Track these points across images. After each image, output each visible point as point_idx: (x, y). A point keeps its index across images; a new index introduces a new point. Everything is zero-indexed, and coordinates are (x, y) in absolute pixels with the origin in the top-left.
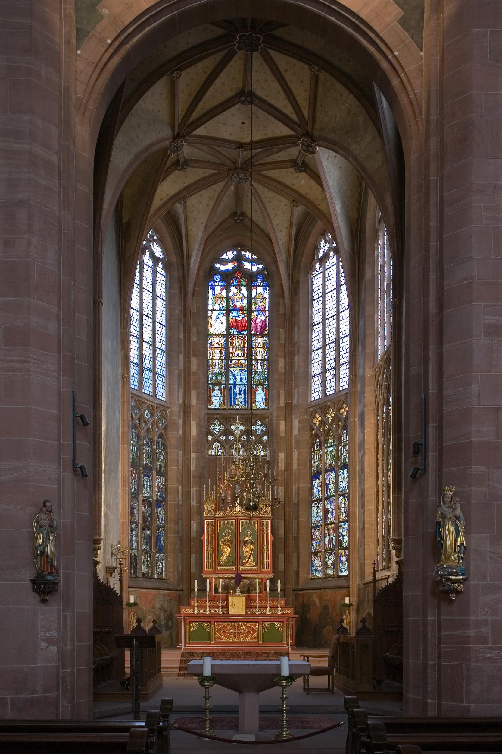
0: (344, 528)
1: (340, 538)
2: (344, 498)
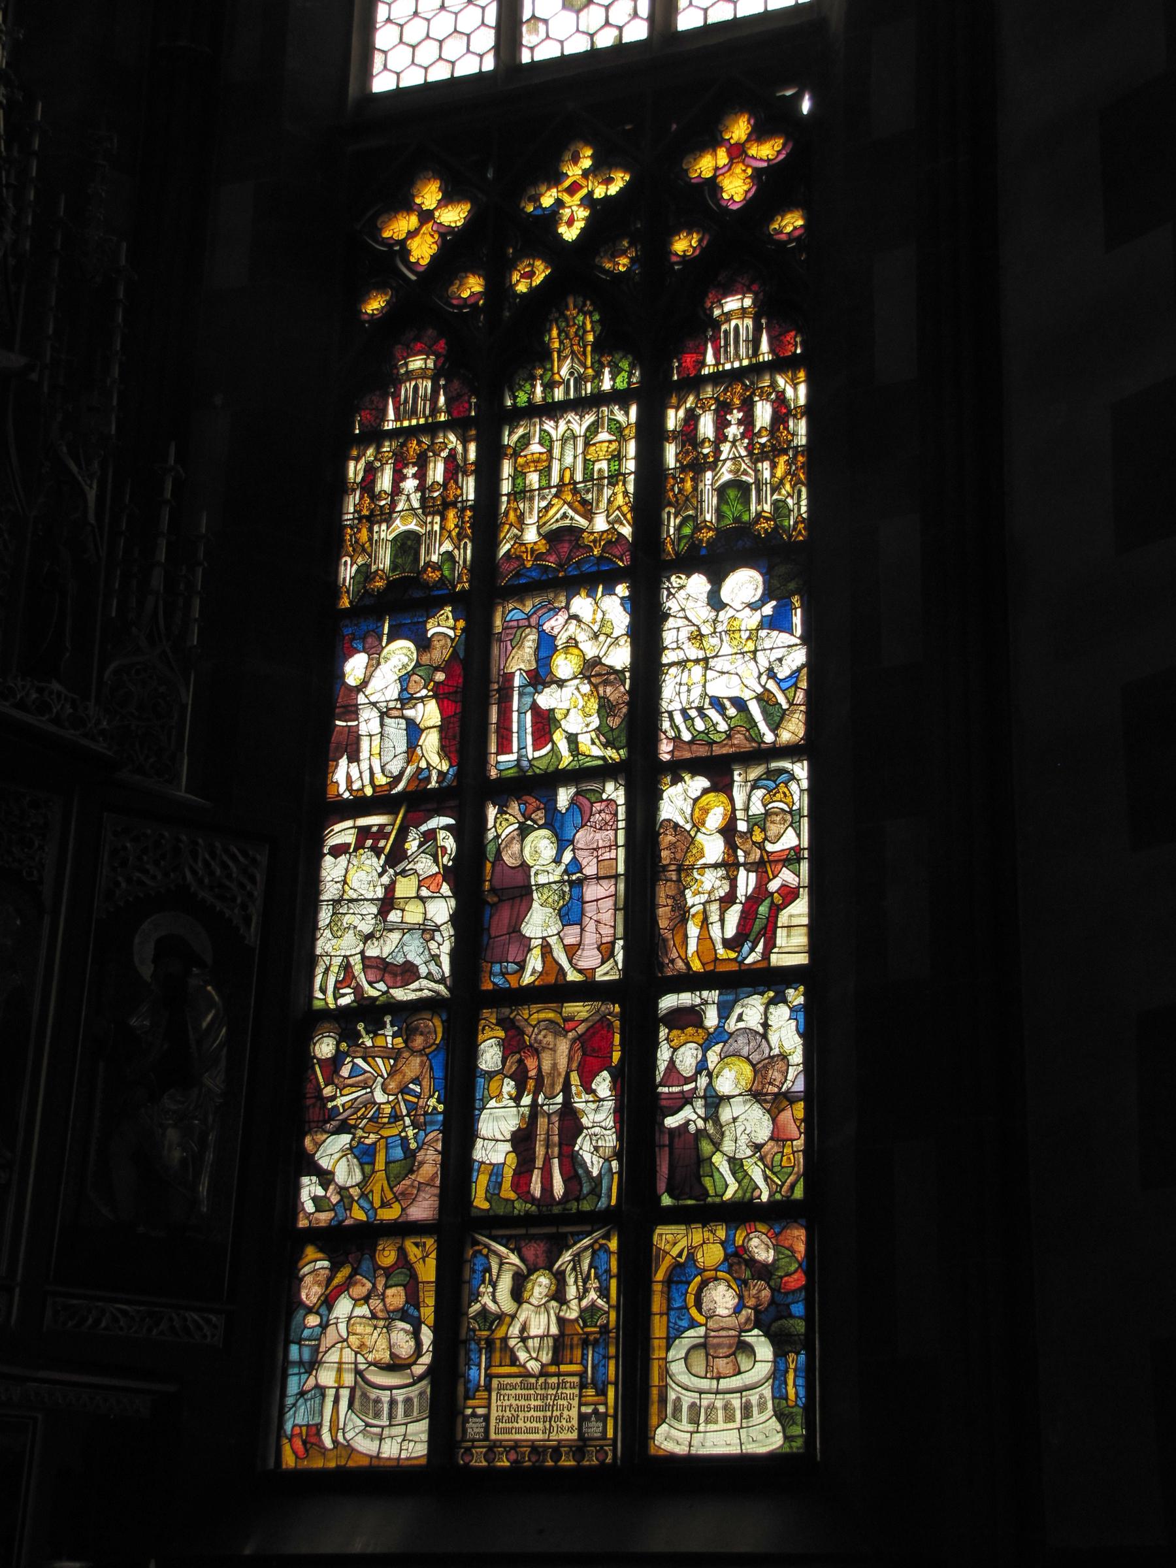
0: (720, 1035)
1: (671, 1122)
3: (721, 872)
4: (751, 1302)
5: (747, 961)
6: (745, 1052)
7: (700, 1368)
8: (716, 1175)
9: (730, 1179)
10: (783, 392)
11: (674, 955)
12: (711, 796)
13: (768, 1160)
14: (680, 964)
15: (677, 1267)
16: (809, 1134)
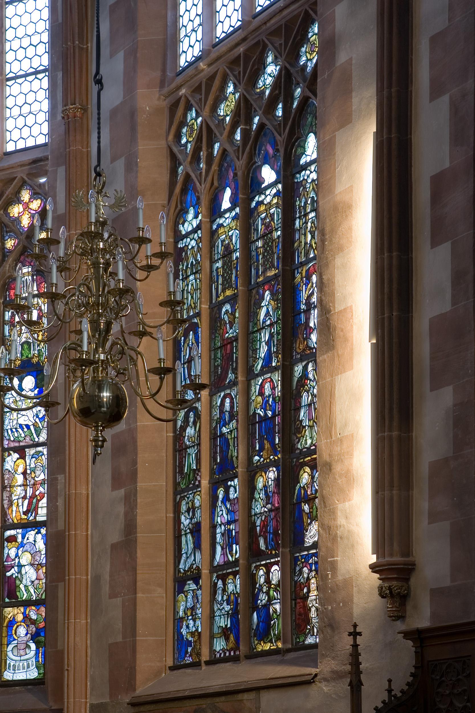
0: (22, 545)
1: (8, 574)
2: (23, 456)
3: (22, 488)
4: (30, 632)
5: (30, 519)
6: (29, 550)
7: (16, 654)
8: (21, 591)
9: (25, 593)
10: (41, 307)
11: (9, 517)
12: (20, 461)
13: (35, 587)
14: (11, 520)
15: (10, 621)
16: (46, 577)
